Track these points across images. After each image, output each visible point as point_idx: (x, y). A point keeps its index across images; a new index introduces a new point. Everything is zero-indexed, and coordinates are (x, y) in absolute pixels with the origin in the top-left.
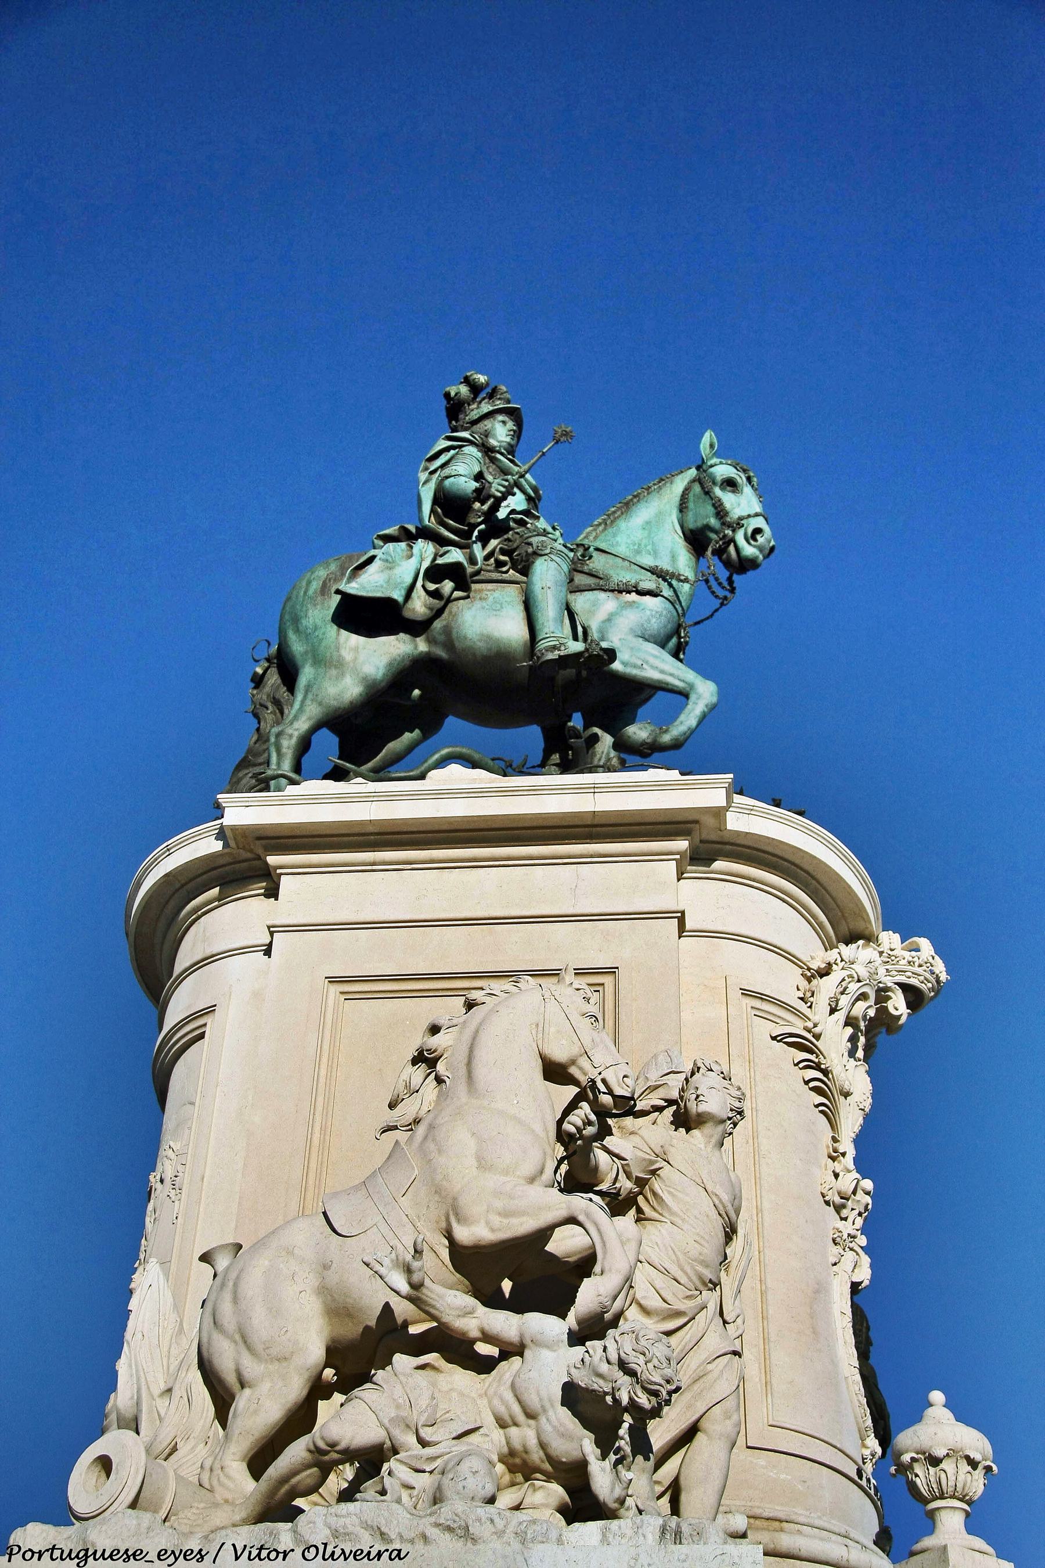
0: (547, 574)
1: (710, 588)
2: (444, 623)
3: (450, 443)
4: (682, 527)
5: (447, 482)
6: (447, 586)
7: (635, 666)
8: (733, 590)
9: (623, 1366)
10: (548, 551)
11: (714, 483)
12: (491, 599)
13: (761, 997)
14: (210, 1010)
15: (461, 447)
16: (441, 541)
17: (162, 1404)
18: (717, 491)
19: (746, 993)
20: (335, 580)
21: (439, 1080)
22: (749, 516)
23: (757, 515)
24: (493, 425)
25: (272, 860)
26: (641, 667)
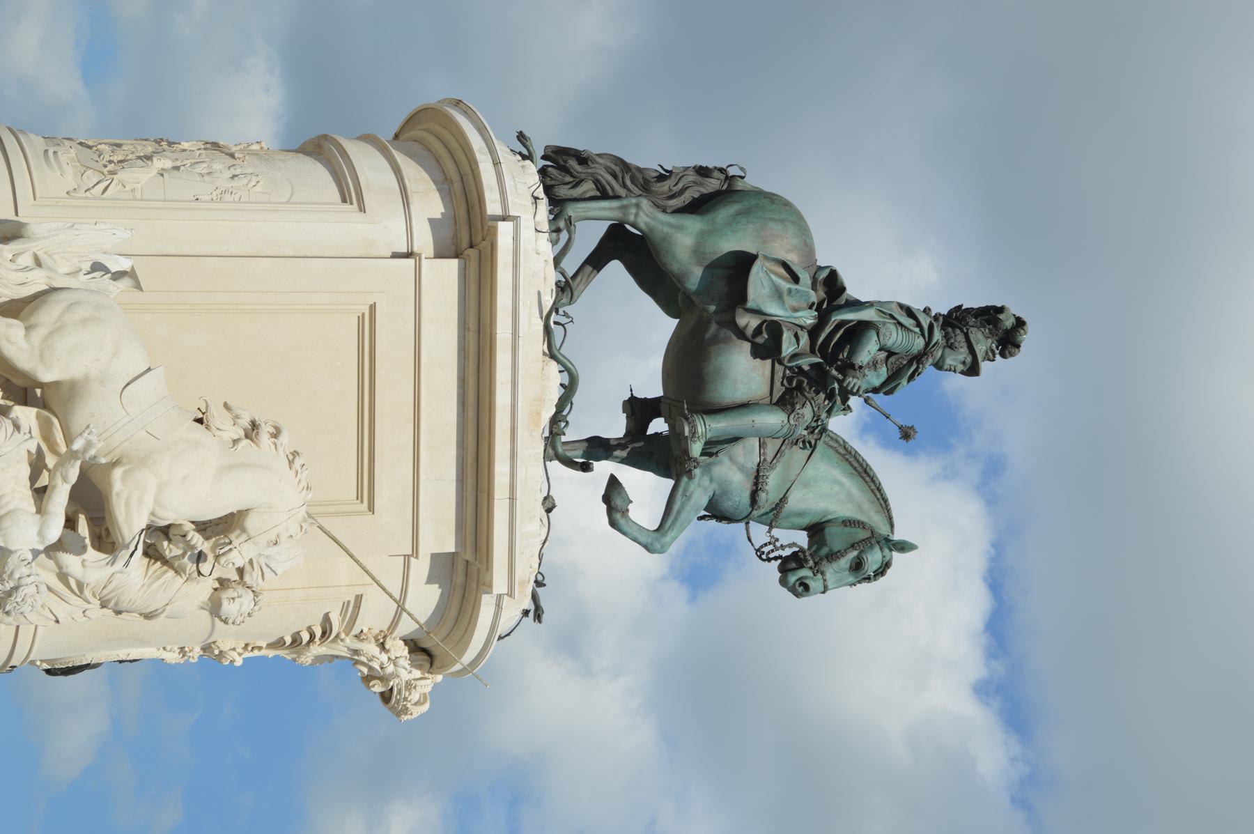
0: (774, 419)
3: (926, 327)
4: (829, 521)
7: (685, 490)
8: (769, 560)
9: (16, 588)
10: (792, 422)
13: (357, 606)
14: (362, 209)
15: (923, 335)
16: (814, 332)
17: (26, 260)
18: (855, 553)
21: (235, 442)
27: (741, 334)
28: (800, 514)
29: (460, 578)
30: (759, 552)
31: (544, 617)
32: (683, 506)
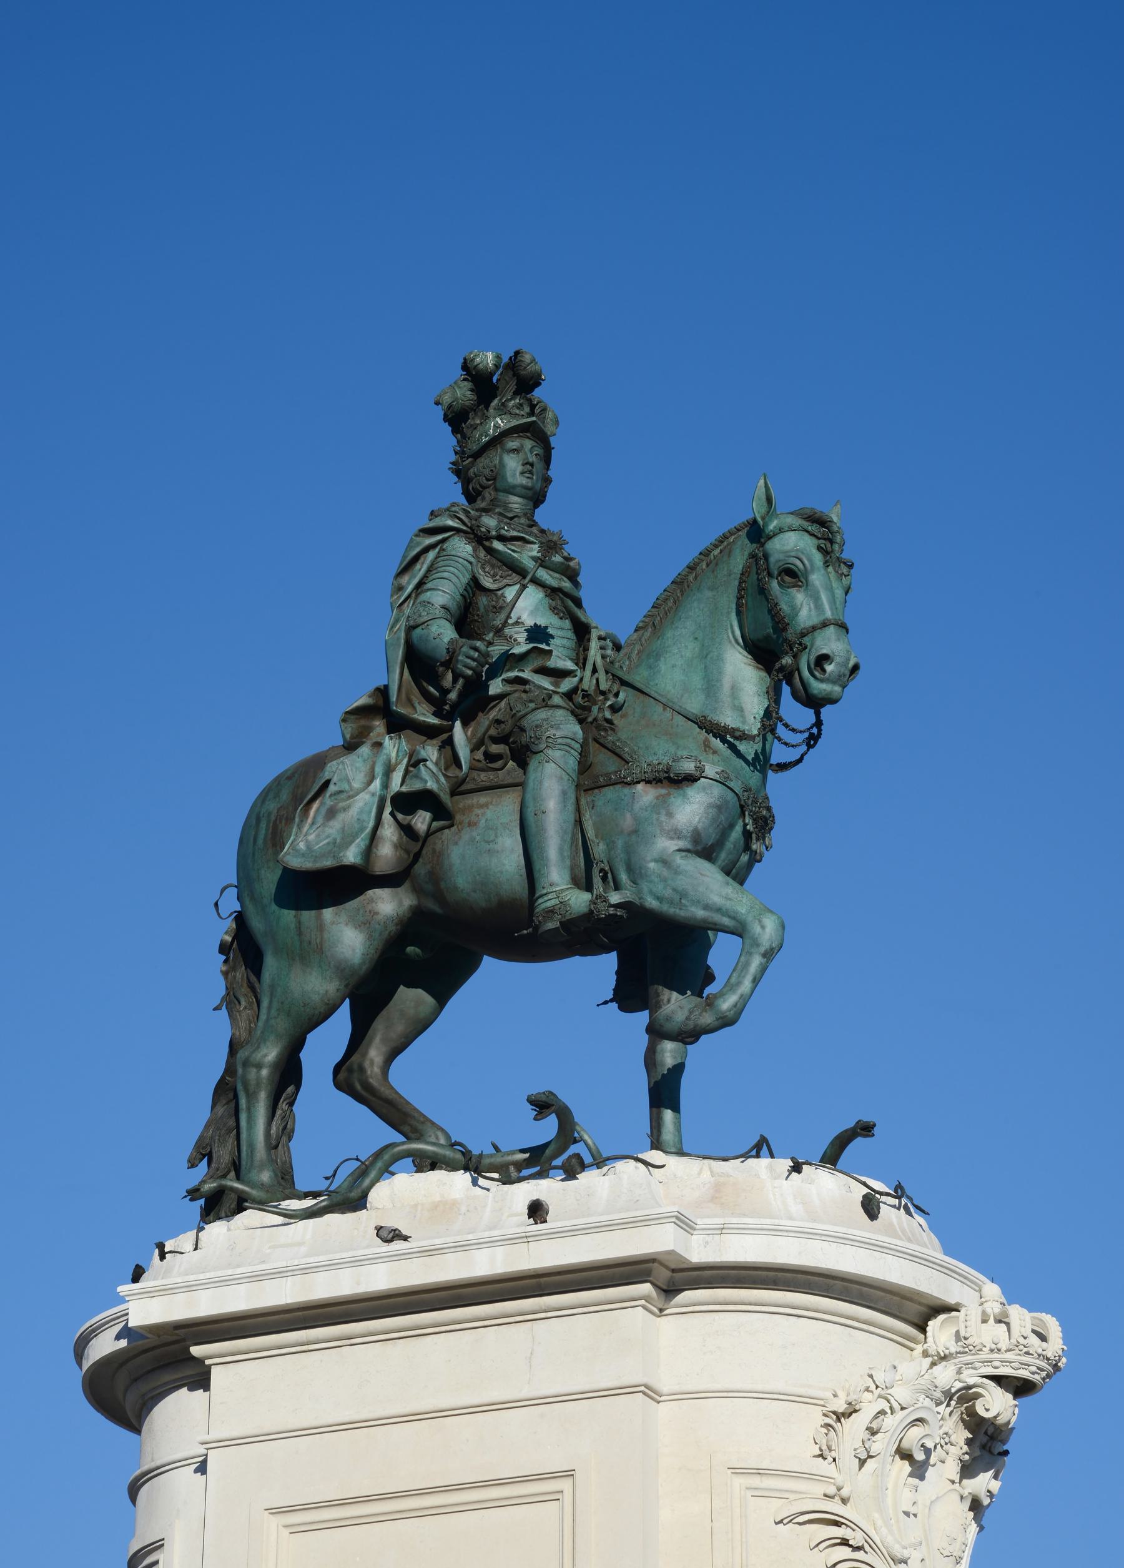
1: (779, 739)
2: (428, 867)
5: (417, 632)
6: (422, 820)
7: (671, 902)
8: (819, 723)
11: (770, 575)
12: (482, 822)
13: (759, 1472)
19: (737, 1471)
20: (287, 819)
22: (814, 628)
23: (825, 625)
24: (501, 459)
25: (196, 1351)
26: (681, 906)
30: (812, 740)
31: (866, 1118)
32: (697, 902)
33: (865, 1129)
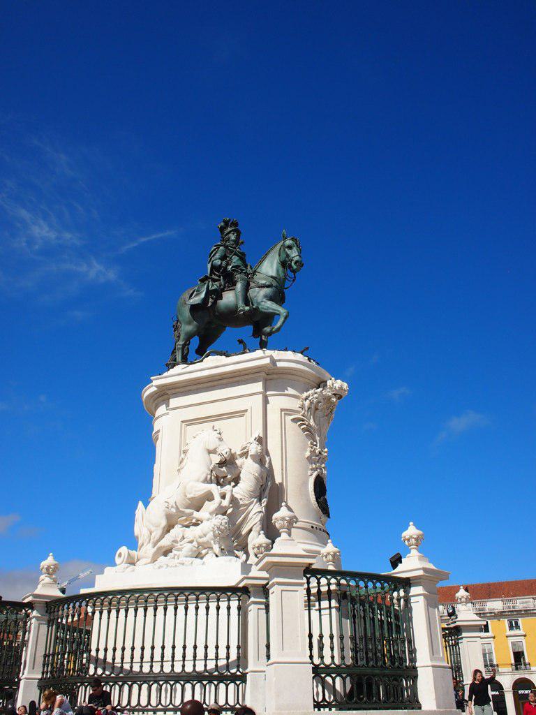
8: (295, 277)
13: (287, 410)
27: (215, 303)
28: (278, 271)
29: (275, 376)
33: (307, 348)
